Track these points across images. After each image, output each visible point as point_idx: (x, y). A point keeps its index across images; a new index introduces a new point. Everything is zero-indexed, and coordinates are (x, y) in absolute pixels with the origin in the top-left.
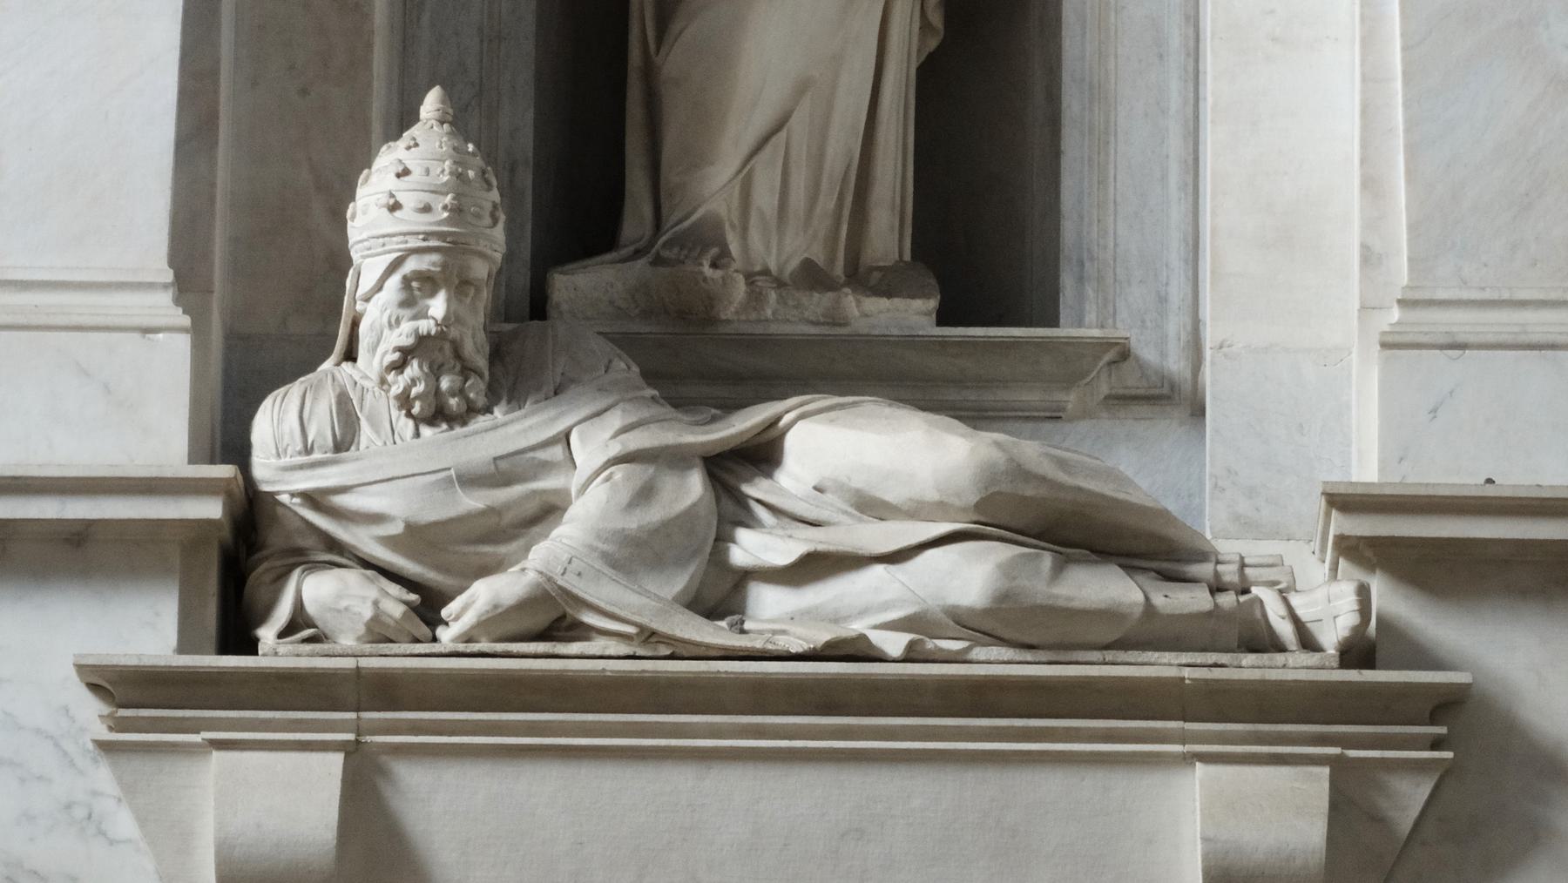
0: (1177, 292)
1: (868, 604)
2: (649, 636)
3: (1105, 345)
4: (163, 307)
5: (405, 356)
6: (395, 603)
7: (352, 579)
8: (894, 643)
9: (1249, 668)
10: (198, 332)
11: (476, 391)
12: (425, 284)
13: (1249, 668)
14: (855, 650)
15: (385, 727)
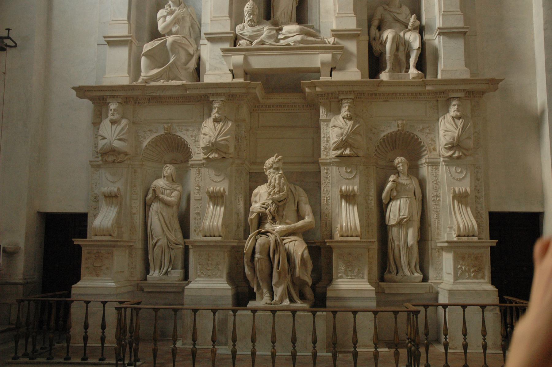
0: (318, 22)
1: (290, 41)
2: (271, 44)
3: (312, 26)
4: (228, 18)
5: (249, 21)
6: (248, 42)
7: (244, 41)
8: (292, 44)
9: (324, 45)
10: (231, 20)
11: (255, 24)
12: (250, 15)
13: (324, 45)
14: (289, 44)
15: (247, 53)
